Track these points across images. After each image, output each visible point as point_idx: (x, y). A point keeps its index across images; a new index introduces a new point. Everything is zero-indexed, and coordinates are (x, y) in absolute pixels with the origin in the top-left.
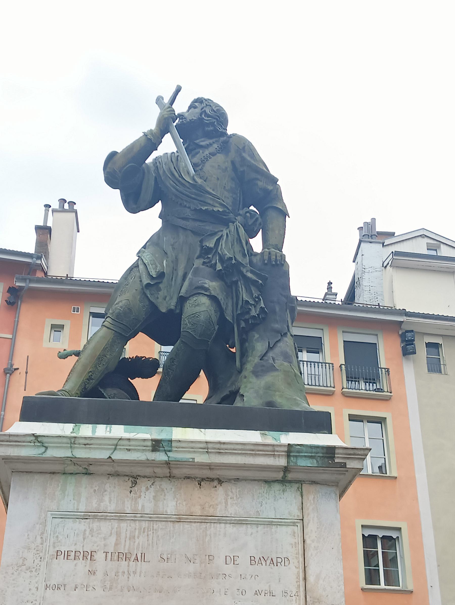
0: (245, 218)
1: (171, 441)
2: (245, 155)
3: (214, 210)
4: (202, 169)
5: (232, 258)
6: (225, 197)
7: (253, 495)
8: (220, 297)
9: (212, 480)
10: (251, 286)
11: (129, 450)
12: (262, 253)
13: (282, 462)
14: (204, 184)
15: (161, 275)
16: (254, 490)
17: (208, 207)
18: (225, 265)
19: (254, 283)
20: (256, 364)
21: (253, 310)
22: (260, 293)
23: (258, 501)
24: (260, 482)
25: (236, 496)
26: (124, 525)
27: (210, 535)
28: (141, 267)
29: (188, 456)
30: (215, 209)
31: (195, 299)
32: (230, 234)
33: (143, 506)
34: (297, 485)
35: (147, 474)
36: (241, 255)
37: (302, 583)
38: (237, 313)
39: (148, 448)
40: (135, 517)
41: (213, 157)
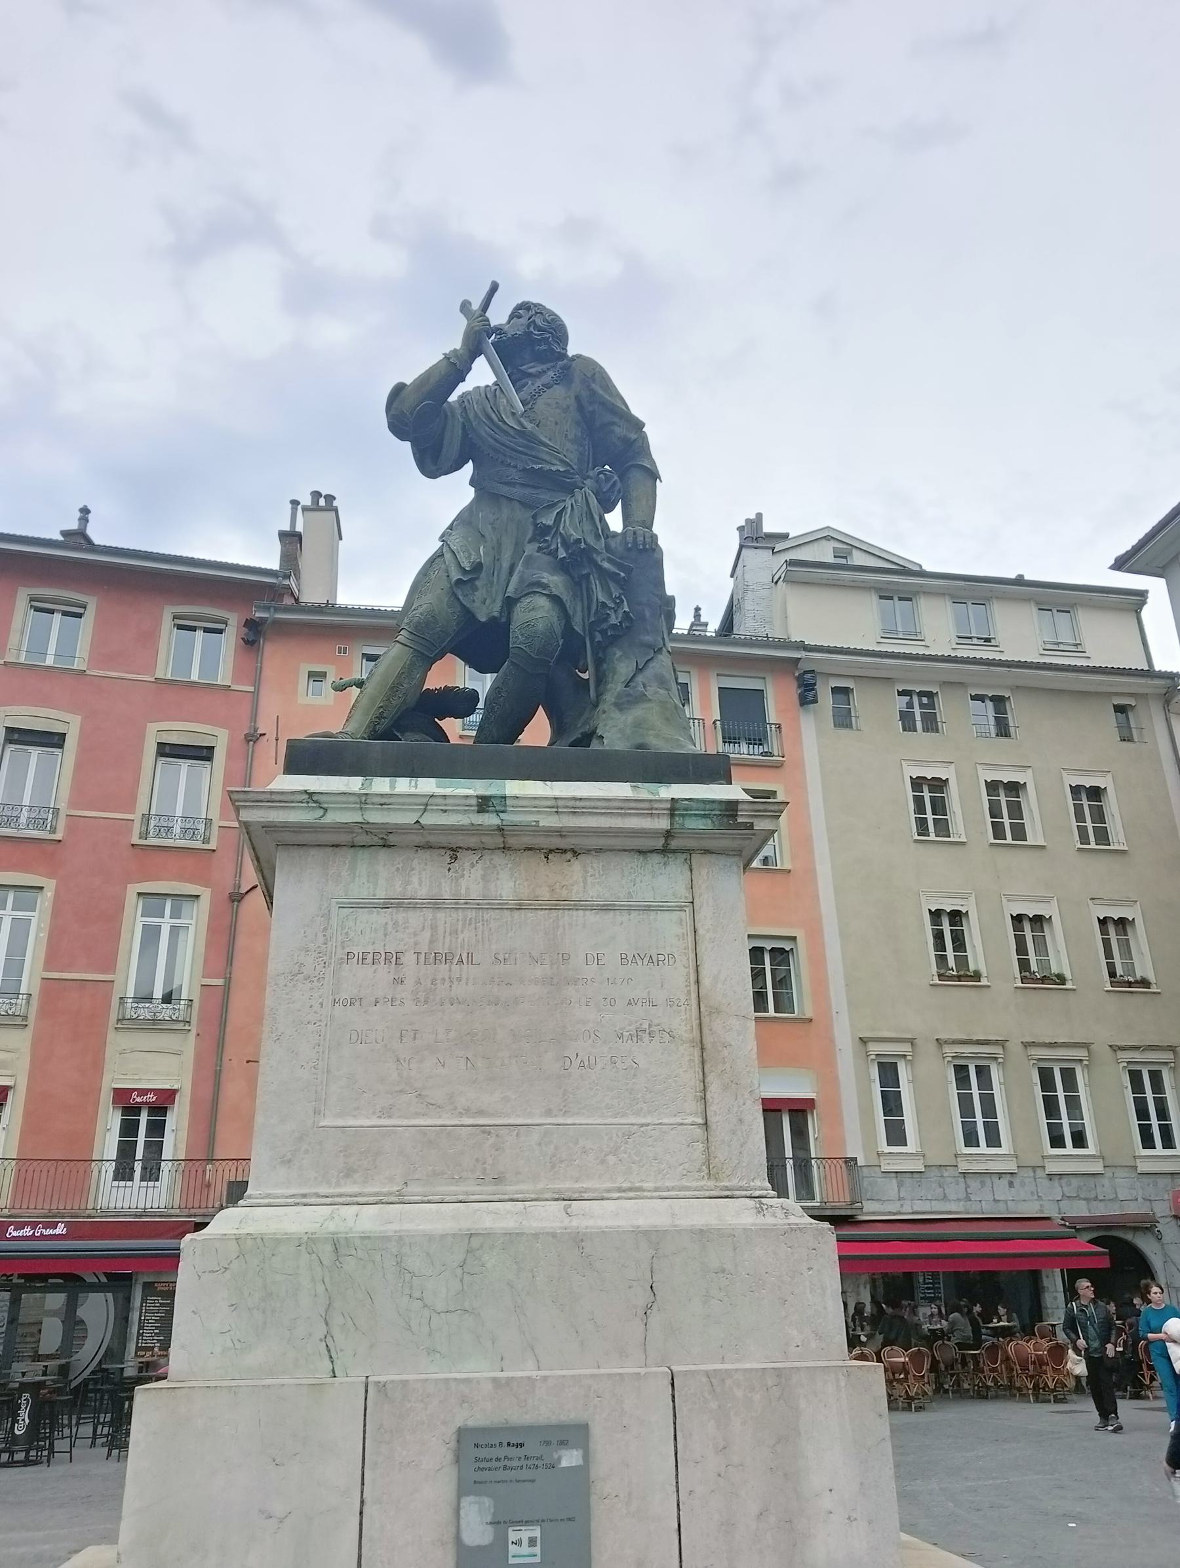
0: (597, 482)
1: (504, 797)
2: (596, 387)
6: (567, 450)
7: (623, 871)
8: (565, 597)
9: (564, 851)
10: (610, 582)
11: (445, 811)
12: (624, 534)
14: (537, 431)
15: (478, 567)
16: (624, 864)
18: (570, 551)
19: (614, 577)
20: (619, 694)
21: (613, 616)
23: (630, 878)
24: (632, 853)
25: (599, 872)
26: (441, 915)
27: (564, 926)
28: (448, 556)
30: (554, 468)
31: (528, 601)
33: (467, 888)
34: (685, 856)
35: (472, 845)
36: (593, 536)
37: (693, 987)
39: (472, 808)
41: (548, 391)
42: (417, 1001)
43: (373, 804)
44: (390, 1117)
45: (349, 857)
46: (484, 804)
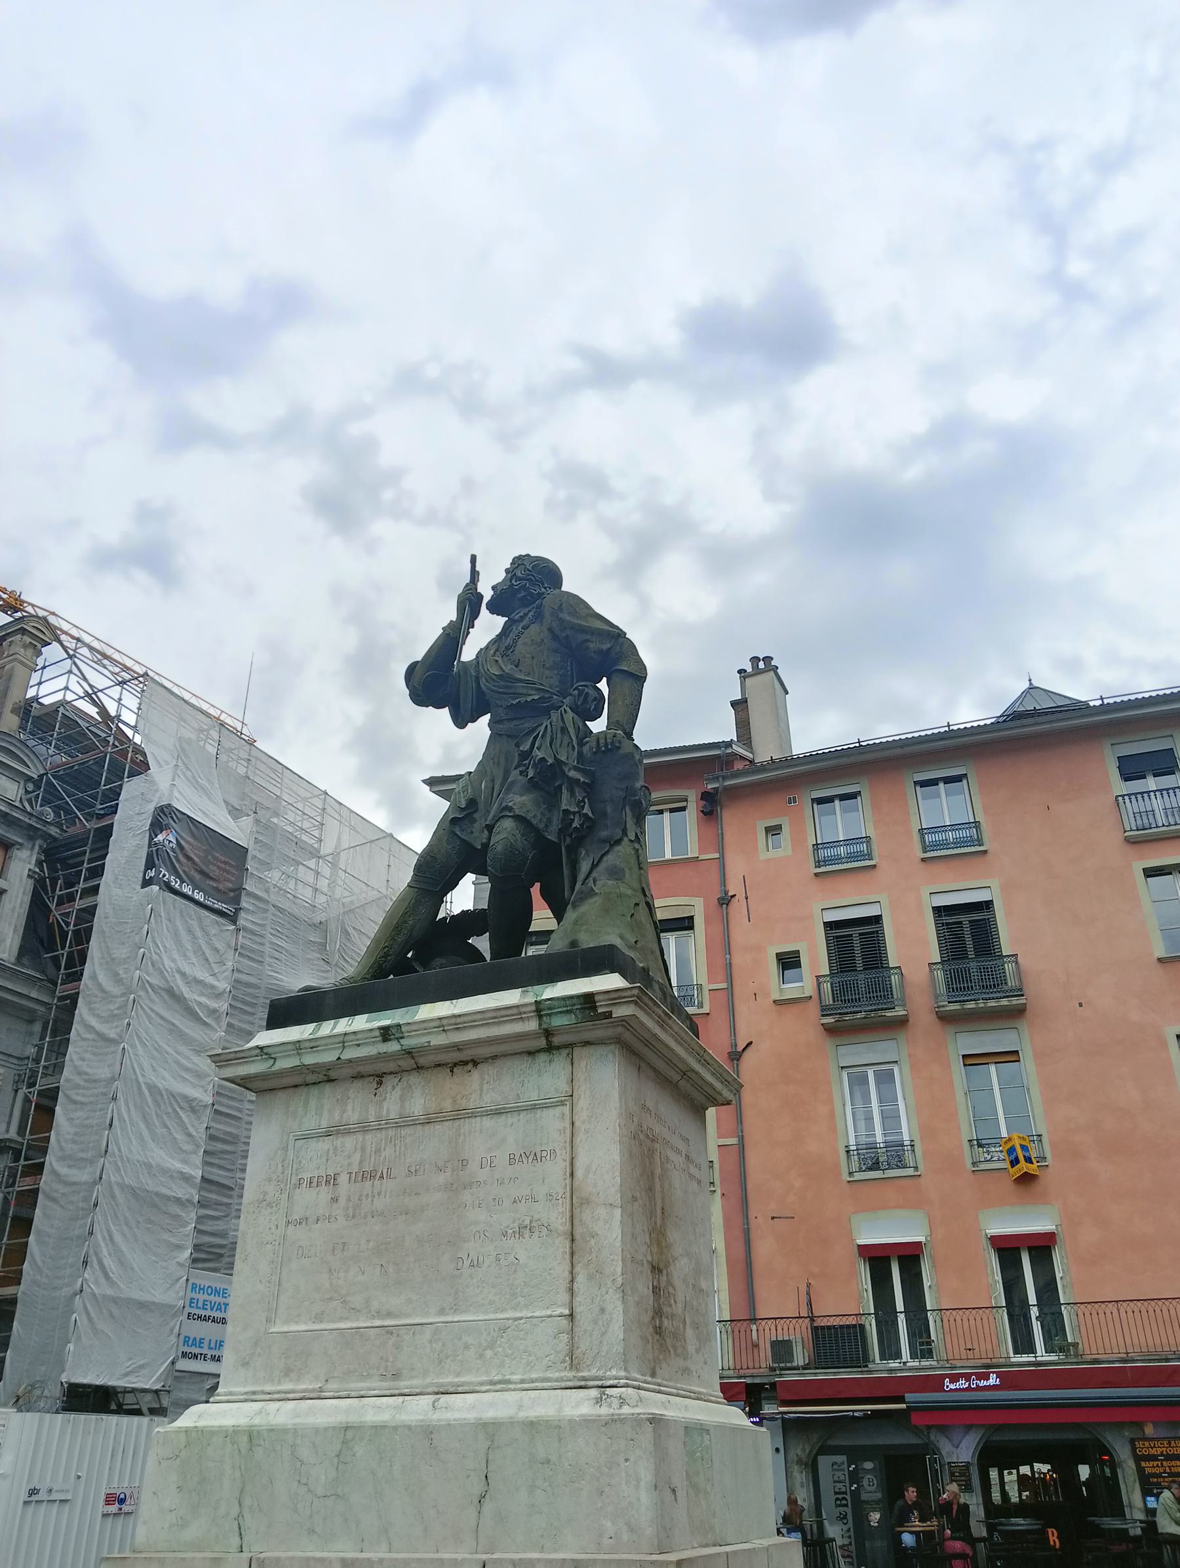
1: (399, 1026)
9: (465, 1063)
11: (359, 1045)
13: (532, 1025)
26: (369, 1137)
29: (422, 1040)
30: (529, 699)
33: (388, 1110)
34: (567, 1051)
35: (392, 1070)
39: (378, 1039)
40: (380, 1125)
42: (347, 1216)
43: (305, 1048)
44: (321, 1322)
45: (304, 1095)
46: (386, 1034)
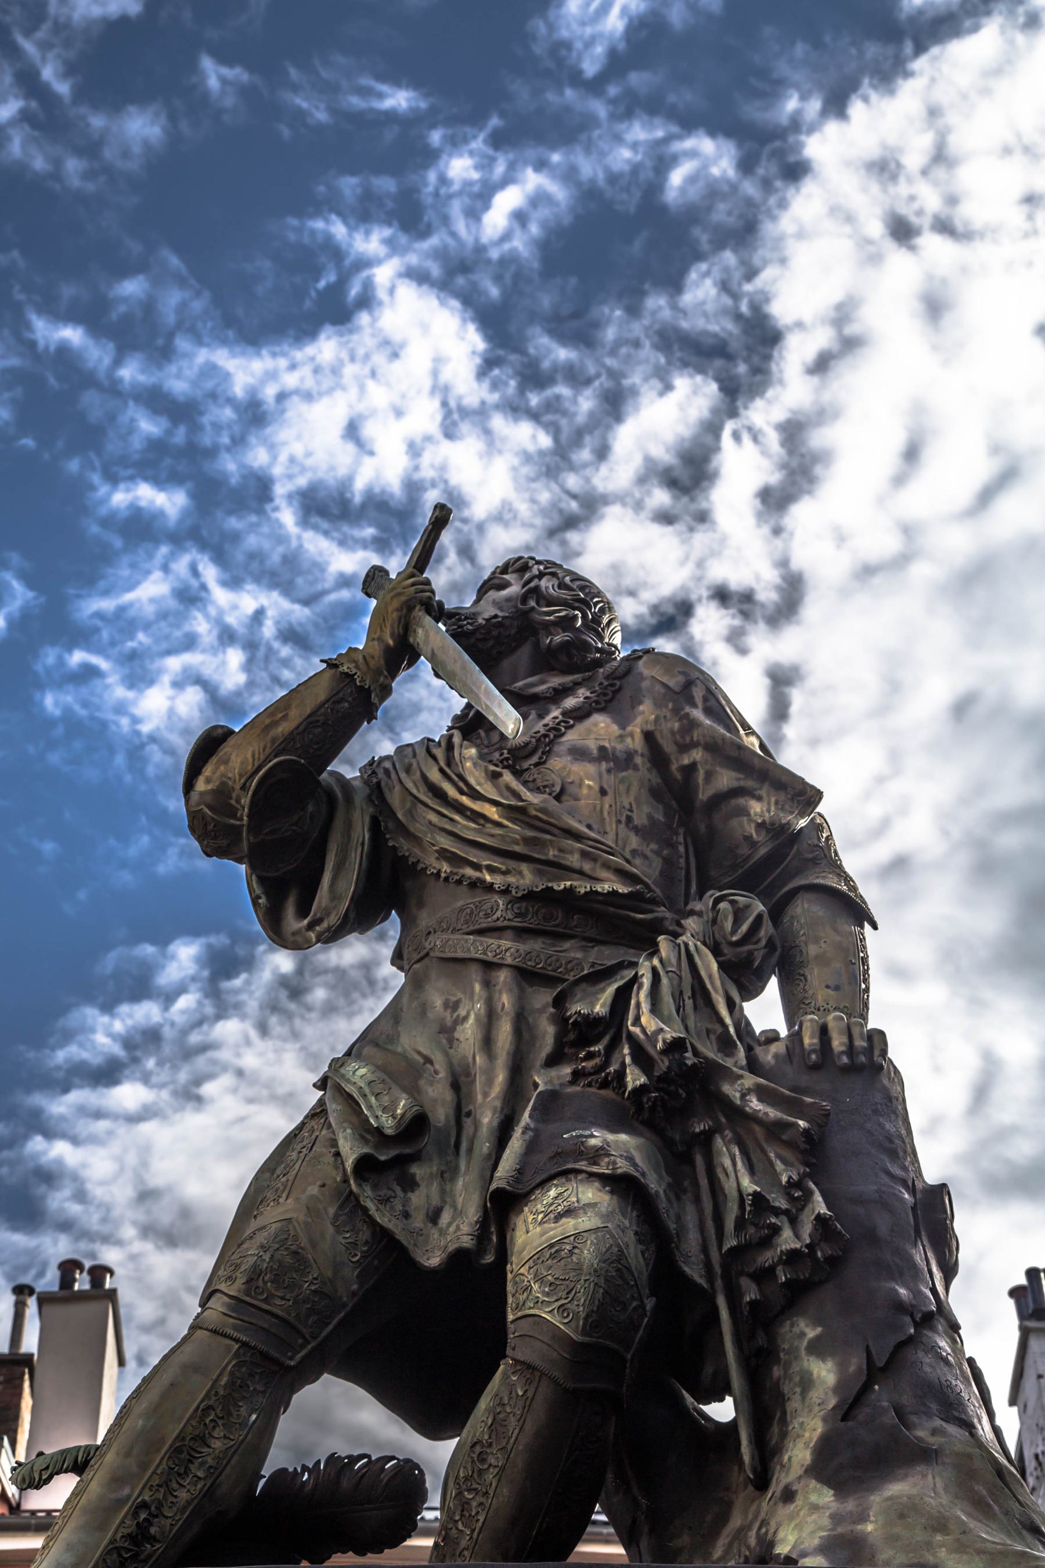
3: (600, 890)
4: (544, 763)
5: (684, 1039)
17: (575, 883)
22: (808, 1170)
31: (553, 1193)
32: (667, 972)
38: (725, 1248)
